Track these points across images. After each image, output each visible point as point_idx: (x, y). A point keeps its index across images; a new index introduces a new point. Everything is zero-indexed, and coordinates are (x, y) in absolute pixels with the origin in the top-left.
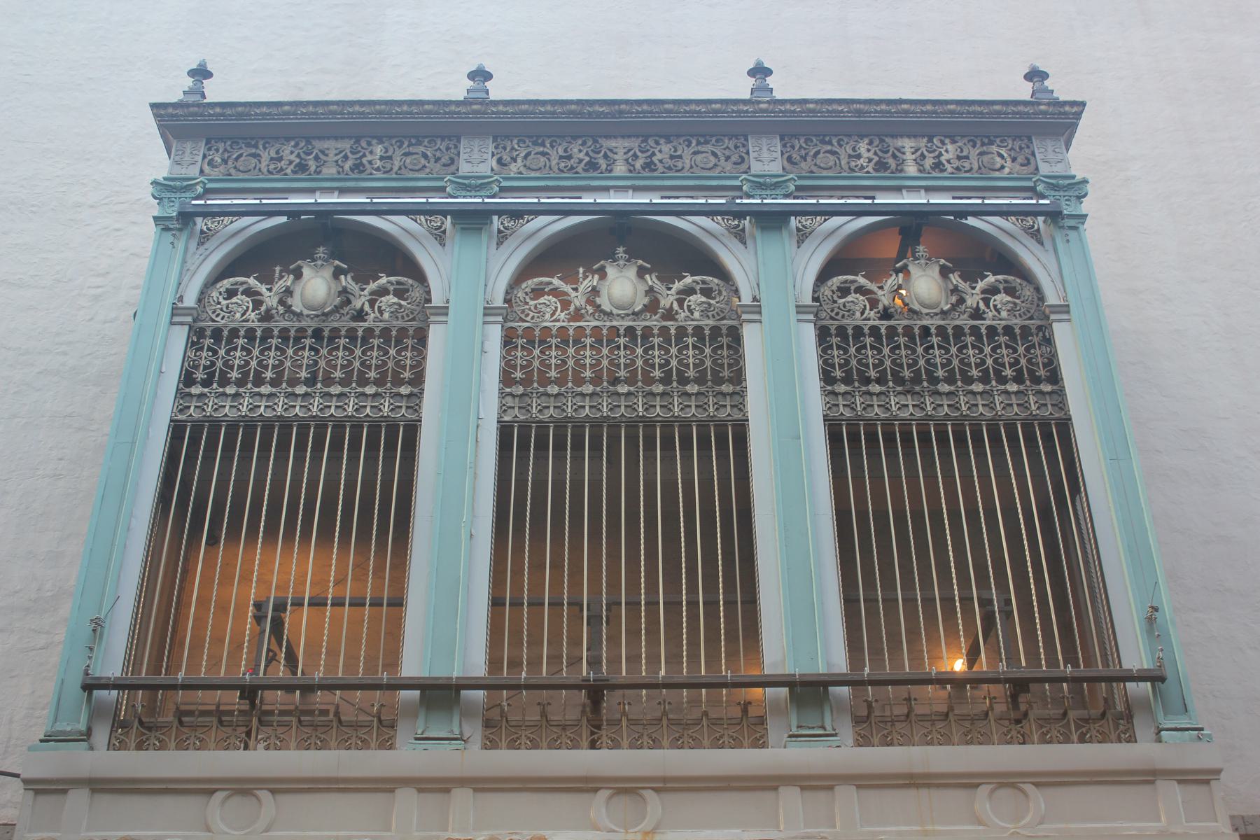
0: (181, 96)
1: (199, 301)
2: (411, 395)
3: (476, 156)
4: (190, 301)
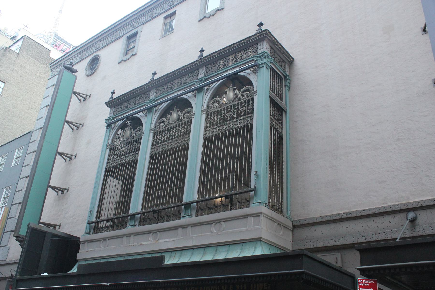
0: (256, 32)
1: (112, 142)
2: (251, 117)
3: (262, 47)
4: (205, 107)
